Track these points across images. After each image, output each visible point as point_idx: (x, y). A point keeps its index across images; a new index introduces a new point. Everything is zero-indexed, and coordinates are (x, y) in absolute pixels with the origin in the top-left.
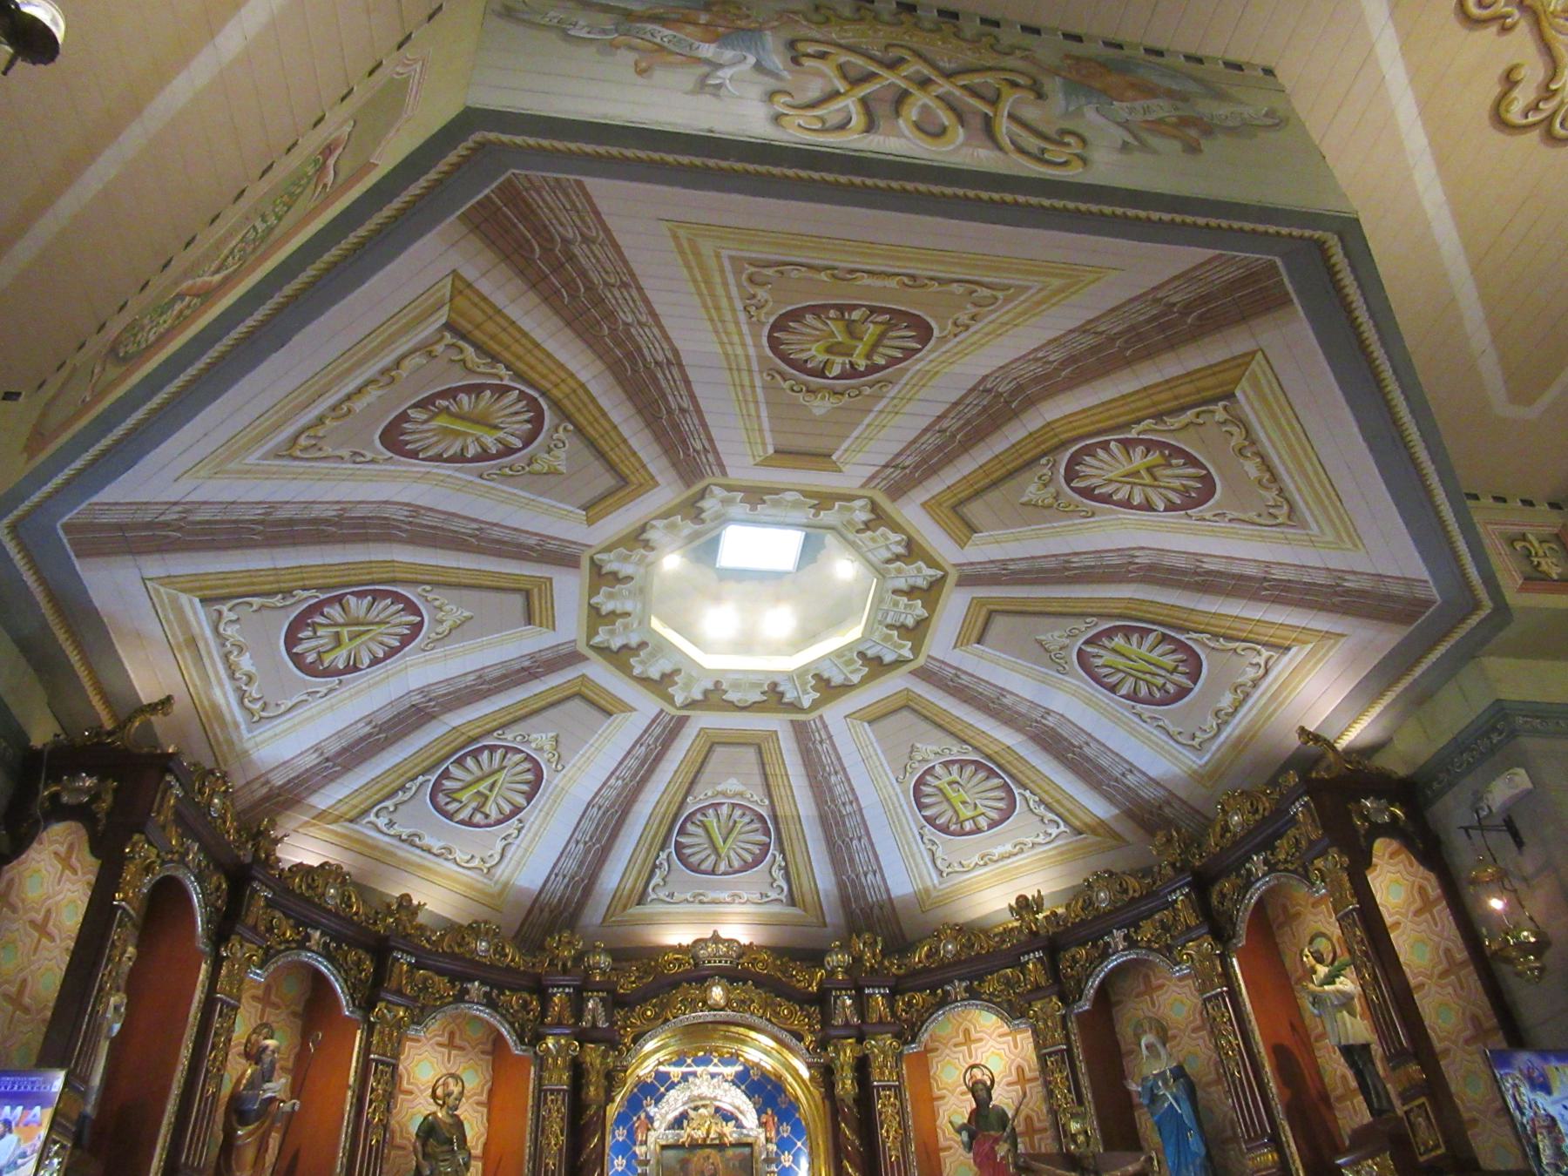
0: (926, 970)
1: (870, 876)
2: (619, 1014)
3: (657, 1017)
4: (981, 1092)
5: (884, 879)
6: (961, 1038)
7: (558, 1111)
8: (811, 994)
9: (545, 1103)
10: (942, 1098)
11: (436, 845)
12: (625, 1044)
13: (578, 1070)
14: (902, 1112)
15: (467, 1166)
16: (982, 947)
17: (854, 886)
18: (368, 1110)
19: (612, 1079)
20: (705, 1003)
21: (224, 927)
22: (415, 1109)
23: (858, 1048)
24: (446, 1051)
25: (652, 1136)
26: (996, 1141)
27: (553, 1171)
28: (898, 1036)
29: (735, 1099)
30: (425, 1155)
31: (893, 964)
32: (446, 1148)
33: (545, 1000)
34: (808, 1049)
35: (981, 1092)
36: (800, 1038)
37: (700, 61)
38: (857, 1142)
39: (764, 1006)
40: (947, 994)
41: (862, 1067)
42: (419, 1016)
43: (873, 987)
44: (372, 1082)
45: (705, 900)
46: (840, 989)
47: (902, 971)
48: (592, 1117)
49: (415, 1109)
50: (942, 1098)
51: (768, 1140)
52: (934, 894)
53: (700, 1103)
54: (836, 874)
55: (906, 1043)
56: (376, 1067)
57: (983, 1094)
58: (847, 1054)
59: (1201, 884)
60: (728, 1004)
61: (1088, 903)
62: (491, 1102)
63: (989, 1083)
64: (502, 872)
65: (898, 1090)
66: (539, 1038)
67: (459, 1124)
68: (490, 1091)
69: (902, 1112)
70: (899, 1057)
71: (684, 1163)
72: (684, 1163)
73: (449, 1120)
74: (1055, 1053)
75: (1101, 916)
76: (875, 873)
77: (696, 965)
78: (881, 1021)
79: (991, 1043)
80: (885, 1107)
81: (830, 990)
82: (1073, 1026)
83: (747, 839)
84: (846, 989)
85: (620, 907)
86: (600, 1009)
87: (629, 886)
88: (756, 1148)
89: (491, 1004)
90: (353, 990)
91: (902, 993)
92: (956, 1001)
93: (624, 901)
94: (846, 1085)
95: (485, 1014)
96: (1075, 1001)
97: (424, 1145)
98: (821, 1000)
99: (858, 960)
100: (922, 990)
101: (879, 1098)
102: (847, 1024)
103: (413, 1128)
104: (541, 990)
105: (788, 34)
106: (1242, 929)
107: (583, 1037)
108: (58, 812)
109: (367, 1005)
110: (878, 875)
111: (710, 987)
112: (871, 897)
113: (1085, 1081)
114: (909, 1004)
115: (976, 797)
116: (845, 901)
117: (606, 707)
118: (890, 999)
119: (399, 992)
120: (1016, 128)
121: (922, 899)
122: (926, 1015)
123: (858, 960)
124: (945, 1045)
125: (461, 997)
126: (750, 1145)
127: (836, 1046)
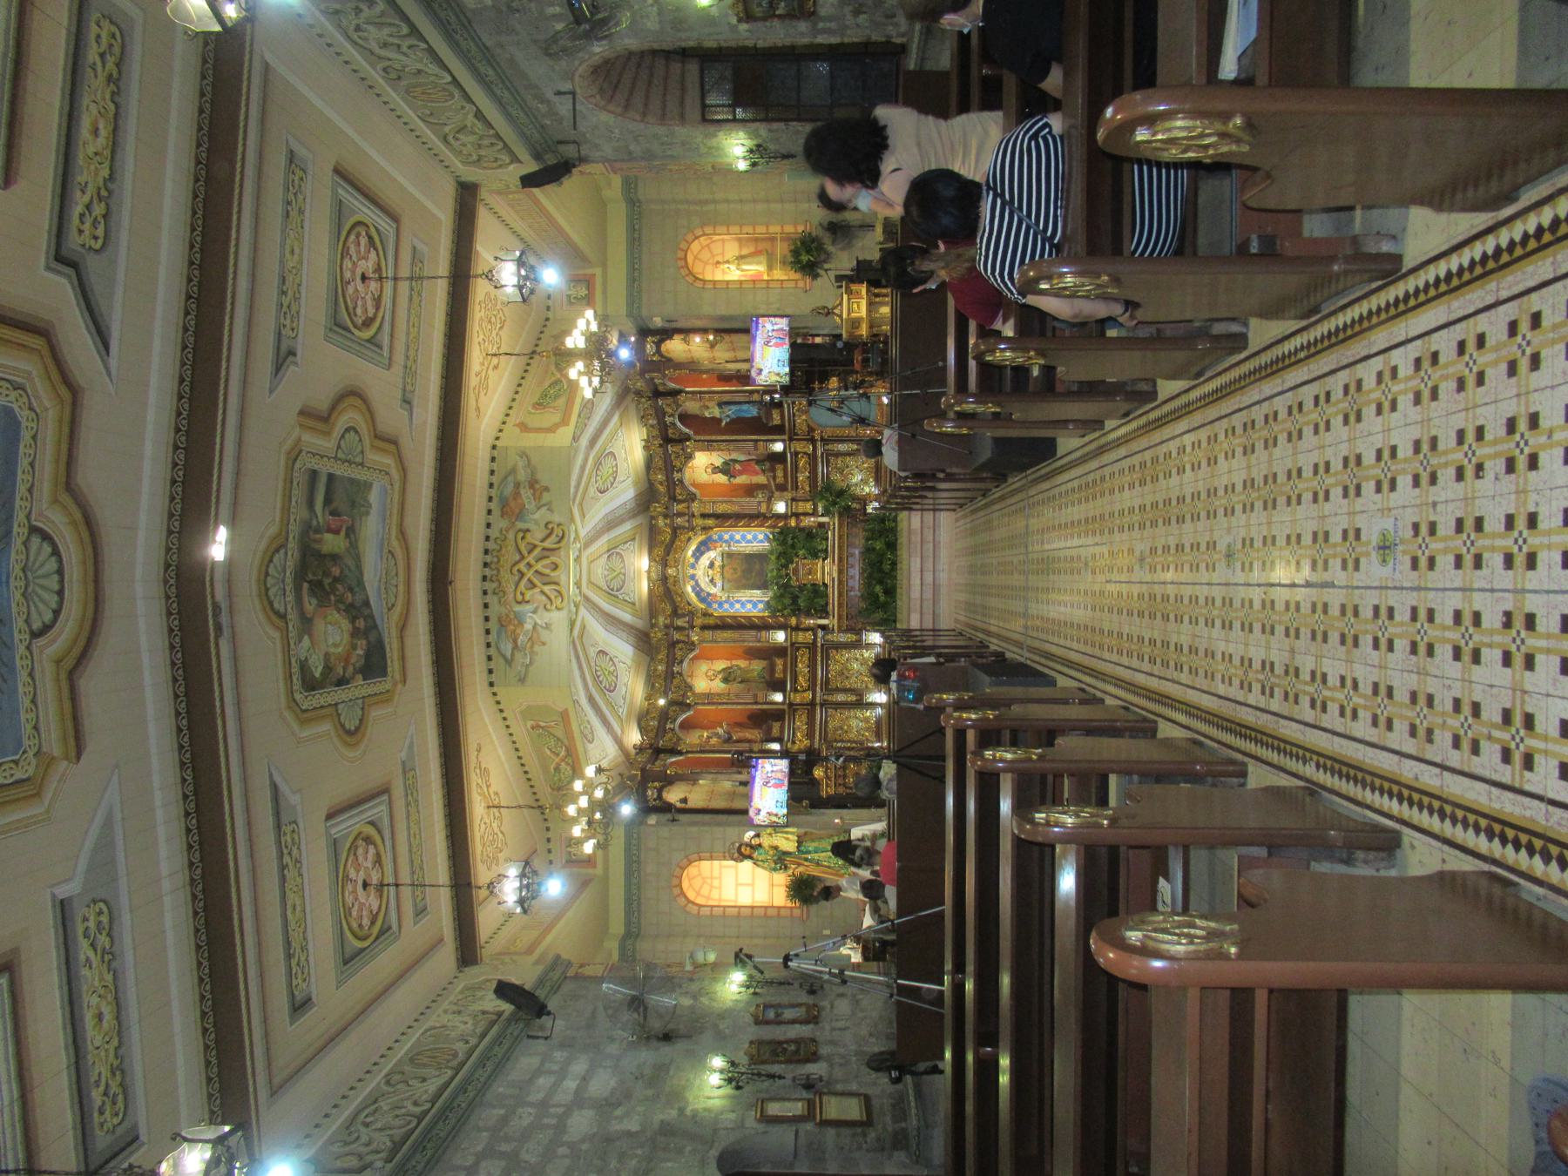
0: (668, 486)
4: (716, 470)
11: (624, 689)
13: (704, 628)
14: (722, 502)
19: (705, 614)
21: (673, 751)
22: (718, 686)
25: (719, 594)
28: (693, 501)
29: (705, 560)
33: (678, 642)
35: (716, 470)
36: (689, 539)
37: (534, 627)
39: (676, 552)
41: (704, 516)
42: (690, 687)
49: (718, 686)
58: (699, 522)
59: (657, 394)
61: (652, 426)
62: (711, 659)
64: (629, 662)
66: (693, 643)
70: (701, 502)
71: (729, 581)
75: (659, 423)
80: (722, 508)
82: (698, 438)
83: (616, 561)
89: (682, 662)
90: (684, 712)
94: (710, 522)
95: (685, 664)
98: (675, 531)
99: (660, 514)
103: (722, 685)
104: (673, 644)
105: (514, 603)
106: (678, 387)
107: (692, 627)
108: (660, 797)
109: (689, 706)
113: (719, 438)
115: (607, 469)
116: (634, 516)
117: (584, 627)
119: (683, 696)
120: (549, 540)
121: (635, 483)
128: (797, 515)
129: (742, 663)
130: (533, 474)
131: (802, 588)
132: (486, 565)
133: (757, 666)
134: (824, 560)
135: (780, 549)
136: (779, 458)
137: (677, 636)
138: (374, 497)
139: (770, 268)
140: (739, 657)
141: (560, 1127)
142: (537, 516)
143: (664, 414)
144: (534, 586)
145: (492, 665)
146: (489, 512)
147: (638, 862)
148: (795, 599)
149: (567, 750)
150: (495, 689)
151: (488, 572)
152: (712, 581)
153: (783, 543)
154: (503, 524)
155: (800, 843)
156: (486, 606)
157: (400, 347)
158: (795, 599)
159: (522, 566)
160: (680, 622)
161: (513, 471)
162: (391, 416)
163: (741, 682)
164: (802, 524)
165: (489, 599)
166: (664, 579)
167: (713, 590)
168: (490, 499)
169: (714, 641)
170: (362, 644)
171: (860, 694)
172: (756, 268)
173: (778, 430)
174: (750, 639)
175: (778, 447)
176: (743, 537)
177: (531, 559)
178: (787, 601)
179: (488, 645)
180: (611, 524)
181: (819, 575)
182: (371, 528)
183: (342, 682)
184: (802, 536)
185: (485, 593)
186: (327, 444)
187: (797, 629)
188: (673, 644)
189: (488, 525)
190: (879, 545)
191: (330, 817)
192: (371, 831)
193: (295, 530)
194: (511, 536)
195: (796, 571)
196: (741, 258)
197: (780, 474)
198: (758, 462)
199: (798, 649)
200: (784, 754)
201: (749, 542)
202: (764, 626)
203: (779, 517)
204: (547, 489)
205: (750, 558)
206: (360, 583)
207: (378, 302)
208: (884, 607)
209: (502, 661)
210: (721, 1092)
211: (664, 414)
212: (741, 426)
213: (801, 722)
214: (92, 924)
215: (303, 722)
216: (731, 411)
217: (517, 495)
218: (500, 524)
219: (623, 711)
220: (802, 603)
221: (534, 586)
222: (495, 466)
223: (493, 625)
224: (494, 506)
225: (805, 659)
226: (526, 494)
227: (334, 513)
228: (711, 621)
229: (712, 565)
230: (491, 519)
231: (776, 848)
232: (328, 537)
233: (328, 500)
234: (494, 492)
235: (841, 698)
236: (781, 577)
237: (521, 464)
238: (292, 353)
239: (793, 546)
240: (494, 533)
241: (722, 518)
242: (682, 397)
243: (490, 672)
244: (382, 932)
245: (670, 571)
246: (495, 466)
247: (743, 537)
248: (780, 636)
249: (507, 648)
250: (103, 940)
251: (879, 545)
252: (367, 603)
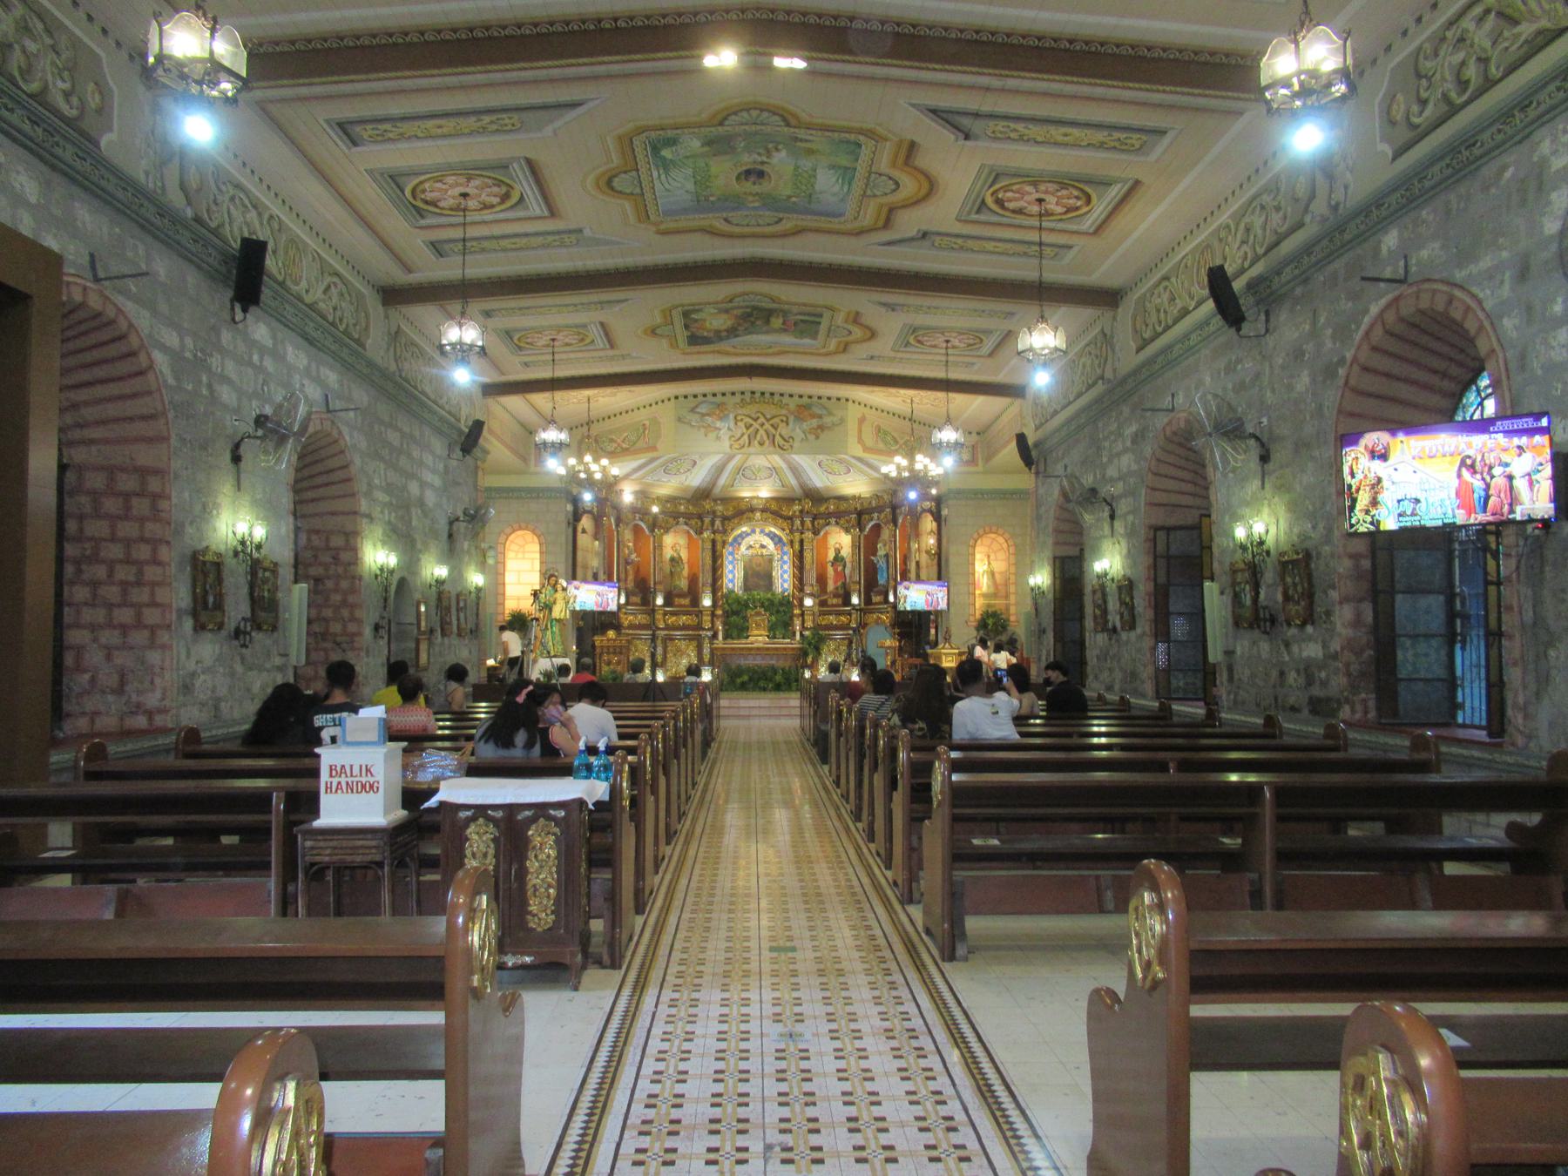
4: (838, 551)
13: (714, 542)
19: (724, 543)
22: (668, 553)
33: (702, 522)
35: (838, 551)
41: (802, 542)
42: (667, 531)
49: (668, 553)
58: (797, 536)
80: (808, 555)
89: (686, 524)
94: (797, 546)
95: (686, 527)
98: (790, 519)
103: (668, 556)
104: (700, 517)
107: (714, 532)
115: (837, 467)
116: (801, 487)
121: (827, 488)
125: (677, 523)
128: (802, 615)
129: (685, 573)
130: (828, 428)
131: (745, 619)
132: (763, 394)
133: (683, 584)
135: (776, 601)
136: (847, 602)
137: (707, 520)
138: (807, 341)
139: (984, 596)
140: (690, 567)
141: (412, 476)
142: (798, 430)
143: (880, 512)
144: (747, 428)
145: (691, 398)
146: (801, 396)
147: (538, 497)
148: (736, 613)
149: (627, 449)
150: (673, 400)
151: (758, 395)
153: (781, 604)
154: (792, 407)
155: (559, 621)
156: (733, 394)
157: (908, 356)
158: (736, 613)
159: (762, 420)
160: (718, 522)
161: (830, 414)
162: (862, 351)
165: (738, 398)
166: (752, 510)
167: (743, 548)
168: (810, 397)
170: (711, 335)
171: (663, 665)
172: (984, 583)
173: (868, 601)
174: (705, 578)
175: (855, 600)
176: (785, 572)
177: (767, 426)
178: (735, 607)
179: (705, 395)
180: (795, 470)
182: (787, 339)
183: (686, 327)
184: (786, 618)
185: (743, 393)
186: (840, 319)
187: (713, 615)
188: (700, 517)
189: (791, 396)
190: (778, 678)
191: (602, 324)
192: (588, 341)
193: (786, 307)
194: (784, 412)
195: (758, 614)
196: (992, 574)
197: (835, 601)
198: (844, 584)
200: (620, 607)
202: (715, 589)
203: (801, 601)
204: (817, 437)
205: (768, 577)
206: (750, 333)
207: (935, 346)
208: (732, 681)
209: (693, 405)
210: (373, 564)
211: (880, 512)
212: (871, 572)
213: (641, 619)
214: (507, 121)
215: (663, 311)
216: (882, 564)
217: (813, 416)
218: (793, 404)
219: (649, 480)
220: (733, 619)
221: (747, 428)
222: (834, 400)
223: (719, 399)
224: (805, 400)
225: (690, 622)
226: (815, 423)
227: (795, 324)
228: (719, 547)
229: (763, 546)
230: (796, 398)
231: (555, 603)
232: (781, 321)
233: (802, 321)
234: (815, 399)
235: (660, 650)
237: (835, 419)
238: (893, 310)
239: (778, 612)
240: (786, 400)
241: (800, 556)
242: (891, 526)
243: (686, 397)
244: (520, 348)
245: (758, 514)
246: (834, 400)
247: (785, 572)
248: (707, 602)
249: (703, 409)
250: (495, 127)
251: (778, 678)
252: (736, 336)
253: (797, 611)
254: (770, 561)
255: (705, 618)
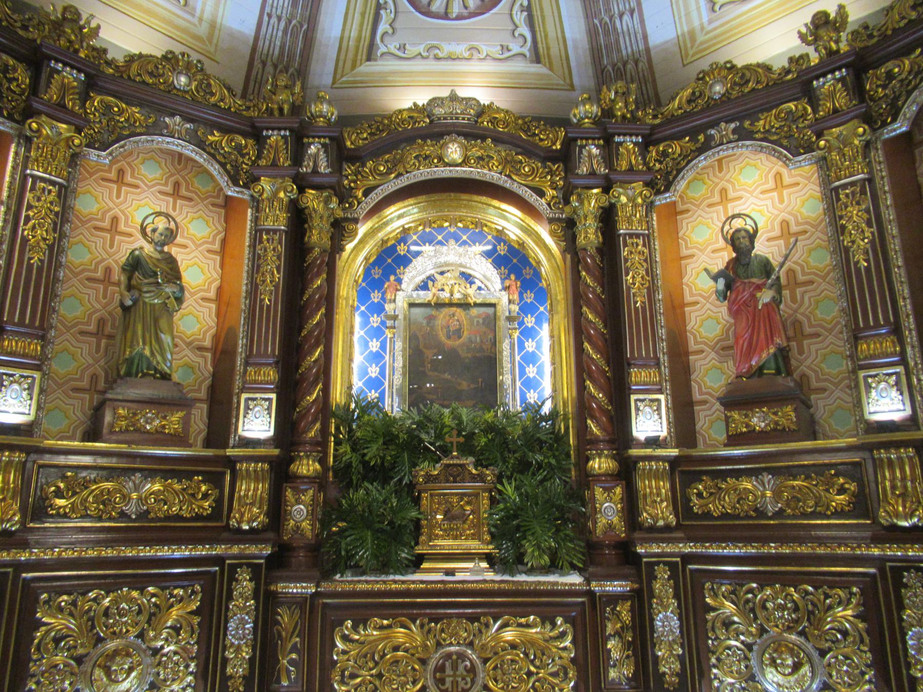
0: (687, 115)
1: (626, 18)
2: (348, 170)
3: (388, 173)
5: (642, 21)
6: (717, 198)
7: (274, 250)
8: (556, 150)
9: (261, 242)
10: (691, 256)
12: (356, 197)
15: (179, 300)
16: (758, 82)
17: (607, 33)
18: (24, 230)
20: (440, 159)
23: (604, 198)
24: (171, 200)
25: (400, 296)
26: (759, 288)
27: (269, 307)
30: (130, 288)
31: (647, 114)
32: (152, 280)
33: (260, 141)
34: (549, 205)
38: (599, 290)
39: (505, 162)
40: (709, 138)
41: (608, 217)
43: (625, 135)
44: (29, 195)
45: (441, 55)
46: (587, 139)
47: (657, 121)
48: (316, 259)
50: (691, 256)
51: (510, 302)
52: (700, 38)
53: (445, 269)
54: (587, 17)
55: (658, 193)
56: (34, 183)
57: (746, 242)
58: (594, 200)
60: (465, 162)
63: (751, 231)
65: (648, 239)
67: (171, 261)
68: (224, 242)
69: (650, 261)
71: (430, 318)
72: (430, 318)
73: (157, 256)
74: (852, 184)
76: (632, 12)
77: (431, 122)
78: (631, 170)
79: (752, 200)
81: (575, 139)
82: (878, 155)
84: (594, 139)
85: (349, 64)
86: (322, 155)
87: (354, 34)
88: (498, 307)
91: (657, 143)
92: (722, 144)
93: (351, 55)
96: (884, 124)
97: (130, 279)
99: (608, 113)
100: (679, 137)
101: (625, 245)
102: (593, 174)
104: (256, 134)
110: (636, 15)
111: (445, 146)
112: (627, 48)
113: (889, 215)
114: (665, 154)
116: (596, 53)
118: (644, 147)
122: (683, 163)
123: (608, 113)
124: (698, 206)
126: (493, 305)
127: (579, 195)
134: (488, 558)
152: (431, 278)
163: (126, 309)
164: (598, 492)
169: (257, 233)
178: (373, 452)
181: (445, 544)
188: (256, 134)
195: (455, 474)
199: (215, 480)
201: (522, 372)
228: (318, 236)
236: (439, 436)
239: (524, 466)
253: (600, 464)
254: (491, 322)
255: (243, 487)
